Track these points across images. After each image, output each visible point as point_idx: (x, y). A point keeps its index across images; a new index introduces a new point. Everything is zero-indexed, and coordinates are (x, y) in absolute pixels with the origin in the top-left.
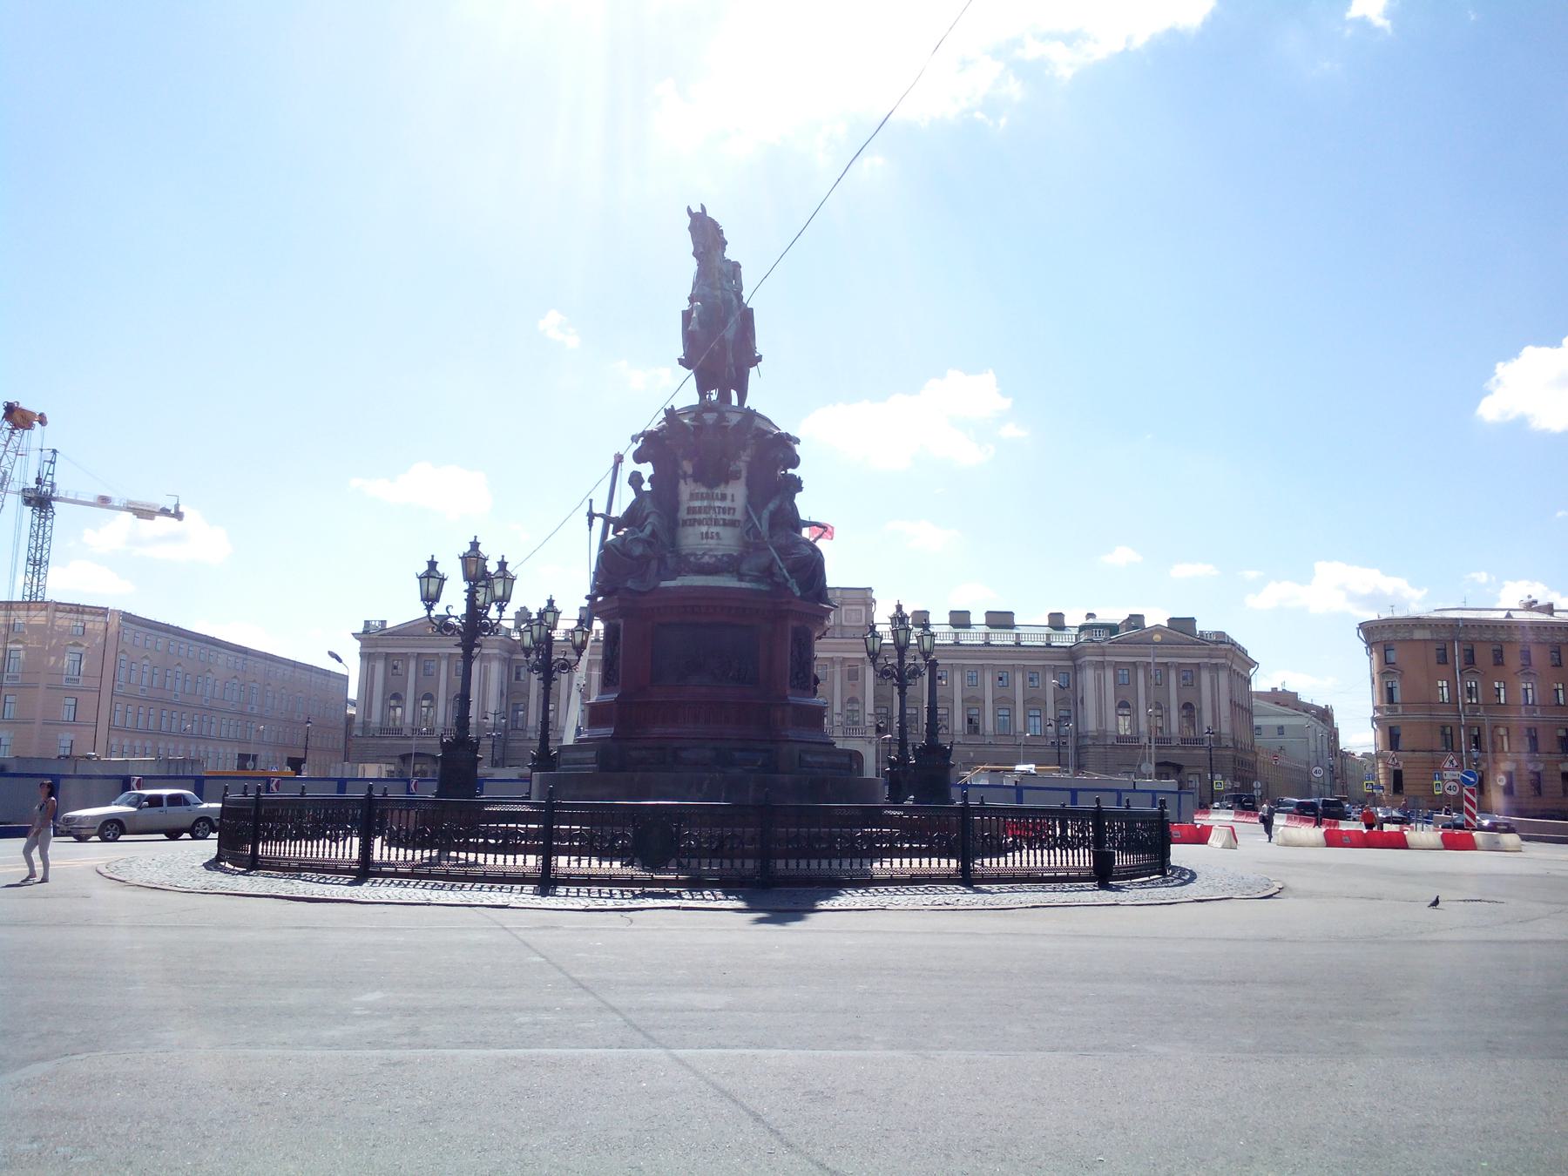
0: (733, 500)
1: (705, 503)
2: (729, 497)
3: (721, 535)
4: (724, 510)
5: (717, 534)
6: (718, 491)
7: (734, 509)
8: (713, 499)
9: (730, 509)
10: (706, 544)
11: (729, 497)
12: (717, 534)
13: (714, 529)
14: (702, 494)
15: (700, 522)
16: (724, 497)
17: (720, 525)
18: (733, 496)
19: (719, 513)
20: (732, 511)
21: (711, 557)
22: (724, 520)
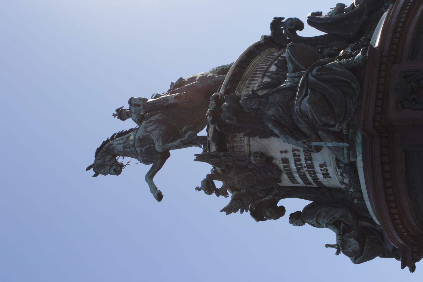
0: (286, 152)
1: (296, 175)
2: (284, 155)
3: (322, 162)
4: (297, 160)
5: (321, 166)
6: (281, 166)
7: (294, 150)
8: (290, 169)
9: (294, 155)
10: (333, 174)
11: (284, 155)
12: (321, 166)
13: (318, 169)
14: (288, 177)
15: (316, 179)
16: (285, 161)
17: (312, 163)
18: (281, 152)
20: (296, 152)
21: (344, 178)
22: (306, 160)
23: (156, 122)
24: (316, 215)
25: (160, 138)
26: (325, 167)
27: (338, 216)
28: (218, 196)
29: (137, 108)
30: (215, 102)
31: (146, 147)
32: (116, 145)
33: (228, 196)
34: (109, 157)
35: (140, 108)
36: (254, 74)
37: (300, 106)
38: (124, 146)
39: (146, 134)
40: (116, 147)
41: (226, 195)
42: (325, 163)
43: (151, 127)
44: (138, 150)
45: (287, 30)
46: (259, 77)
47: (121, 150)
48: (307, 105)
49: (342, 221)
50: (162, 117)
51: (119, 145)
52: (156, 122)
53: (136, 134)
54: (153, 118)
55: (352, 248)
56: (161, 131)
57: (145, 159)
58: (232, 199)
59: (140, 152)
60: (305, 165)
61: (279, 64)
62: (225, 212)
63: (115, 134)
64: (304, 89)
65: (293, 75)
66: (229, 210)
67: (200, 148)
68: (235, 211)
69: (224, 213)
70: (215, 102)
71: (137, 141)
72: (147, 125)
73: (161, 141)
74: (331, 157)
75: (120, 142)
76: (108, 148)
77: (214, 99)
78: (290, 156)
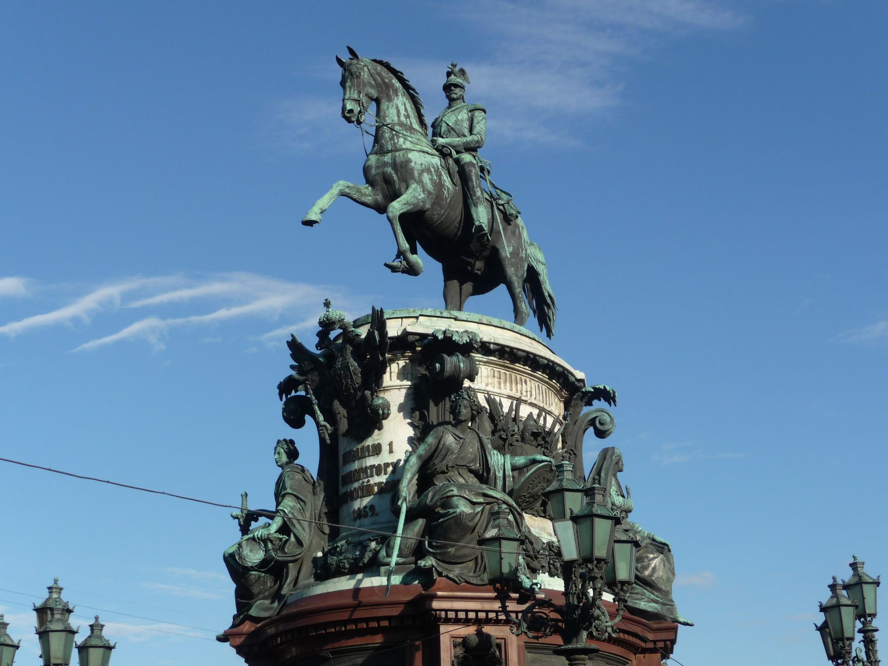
0: (391, 451)
3: (377, 509)
6: (369, 442)
9: (387, 465)
11: (385, 448)
16: (377, 450)
18: (391, 444)
19: (372, 476)
23: (439, 185)
24: (295, 493)
25: (409, 208)
26: (370, 514)
27: (296, 531)
28: (317, 335)
29: (466, 125)
30: (465, 342)
31: (394, 175)
32: (396, 104)
33: (318, 350)
34: (374, 93)
35: (466, 132)
36: (516, 379)
37: (457, 496)
38: (394, 125)
39: (416, 174)
40: (393, 106)
41: (318, 346)
42: (377, 515)
43: (430, 179)
44: (388, 158)
45: (594, 416)
46: (511, 390)
47: (387, 118)
48: (458, 511)
49: (289, 537)
50: (447, 196)
51: (395, 112)
52: (439, 185)
53: (417, 151)
54: (445, 178)
55: (249, 554)
56: (421, 204)
57: (373, 169)
58: (314, 355)
59: (384, 161)
60: (372, 482)
61: (532, 423)
62: (292, 340)
63: (417, 93)
64: (481, 500)
65: (508, 467)
66: (295, 346)
67: (396, 256)
68: (293, 356)
69: (290, 339)
70: (465, 342)
71: (404, 156)
72: (432, 170)
73: (405, 210)
74: (385, 525)
75: (403, 112)
76: (388, 86)
77: (470, 340)
78: (385, 458)
